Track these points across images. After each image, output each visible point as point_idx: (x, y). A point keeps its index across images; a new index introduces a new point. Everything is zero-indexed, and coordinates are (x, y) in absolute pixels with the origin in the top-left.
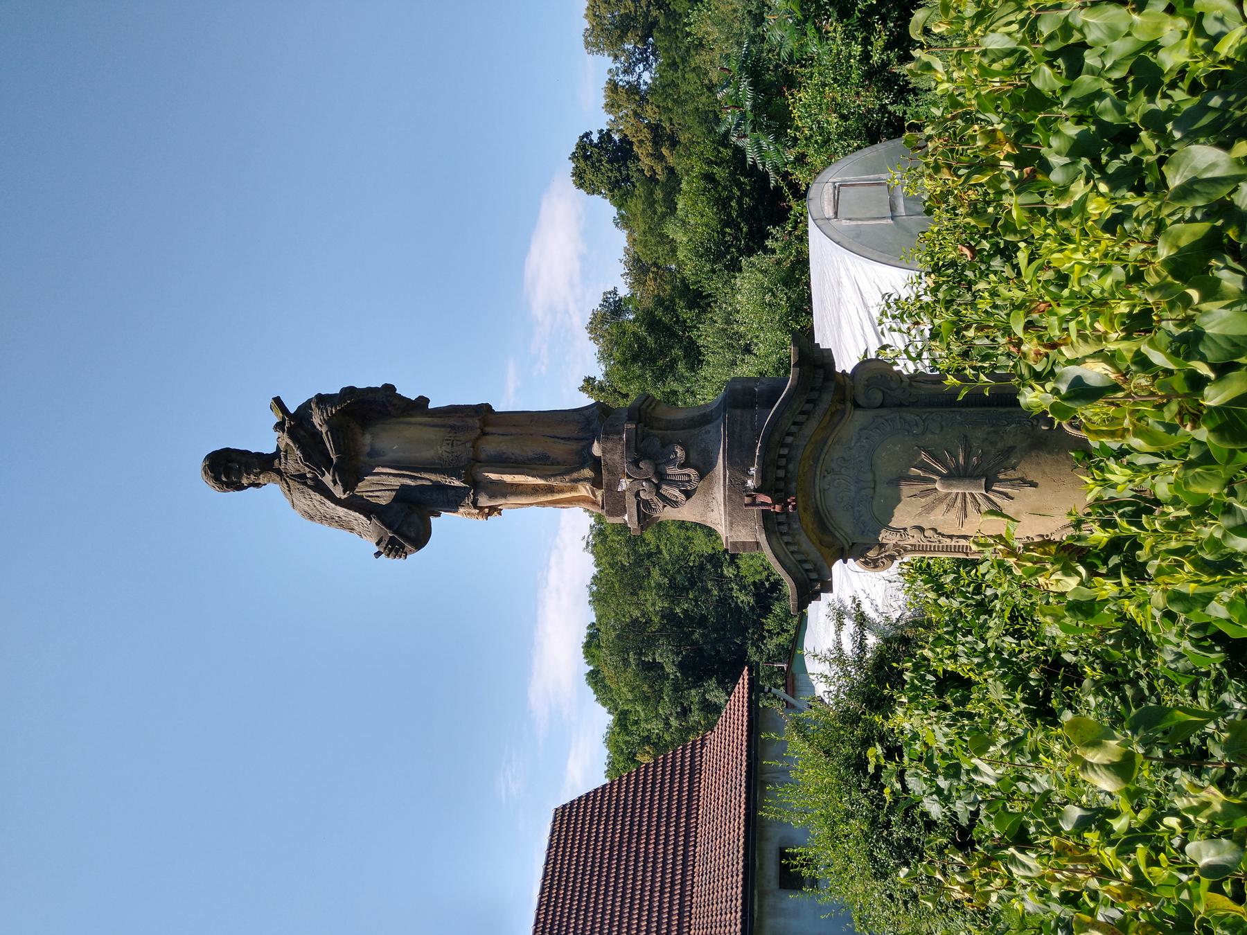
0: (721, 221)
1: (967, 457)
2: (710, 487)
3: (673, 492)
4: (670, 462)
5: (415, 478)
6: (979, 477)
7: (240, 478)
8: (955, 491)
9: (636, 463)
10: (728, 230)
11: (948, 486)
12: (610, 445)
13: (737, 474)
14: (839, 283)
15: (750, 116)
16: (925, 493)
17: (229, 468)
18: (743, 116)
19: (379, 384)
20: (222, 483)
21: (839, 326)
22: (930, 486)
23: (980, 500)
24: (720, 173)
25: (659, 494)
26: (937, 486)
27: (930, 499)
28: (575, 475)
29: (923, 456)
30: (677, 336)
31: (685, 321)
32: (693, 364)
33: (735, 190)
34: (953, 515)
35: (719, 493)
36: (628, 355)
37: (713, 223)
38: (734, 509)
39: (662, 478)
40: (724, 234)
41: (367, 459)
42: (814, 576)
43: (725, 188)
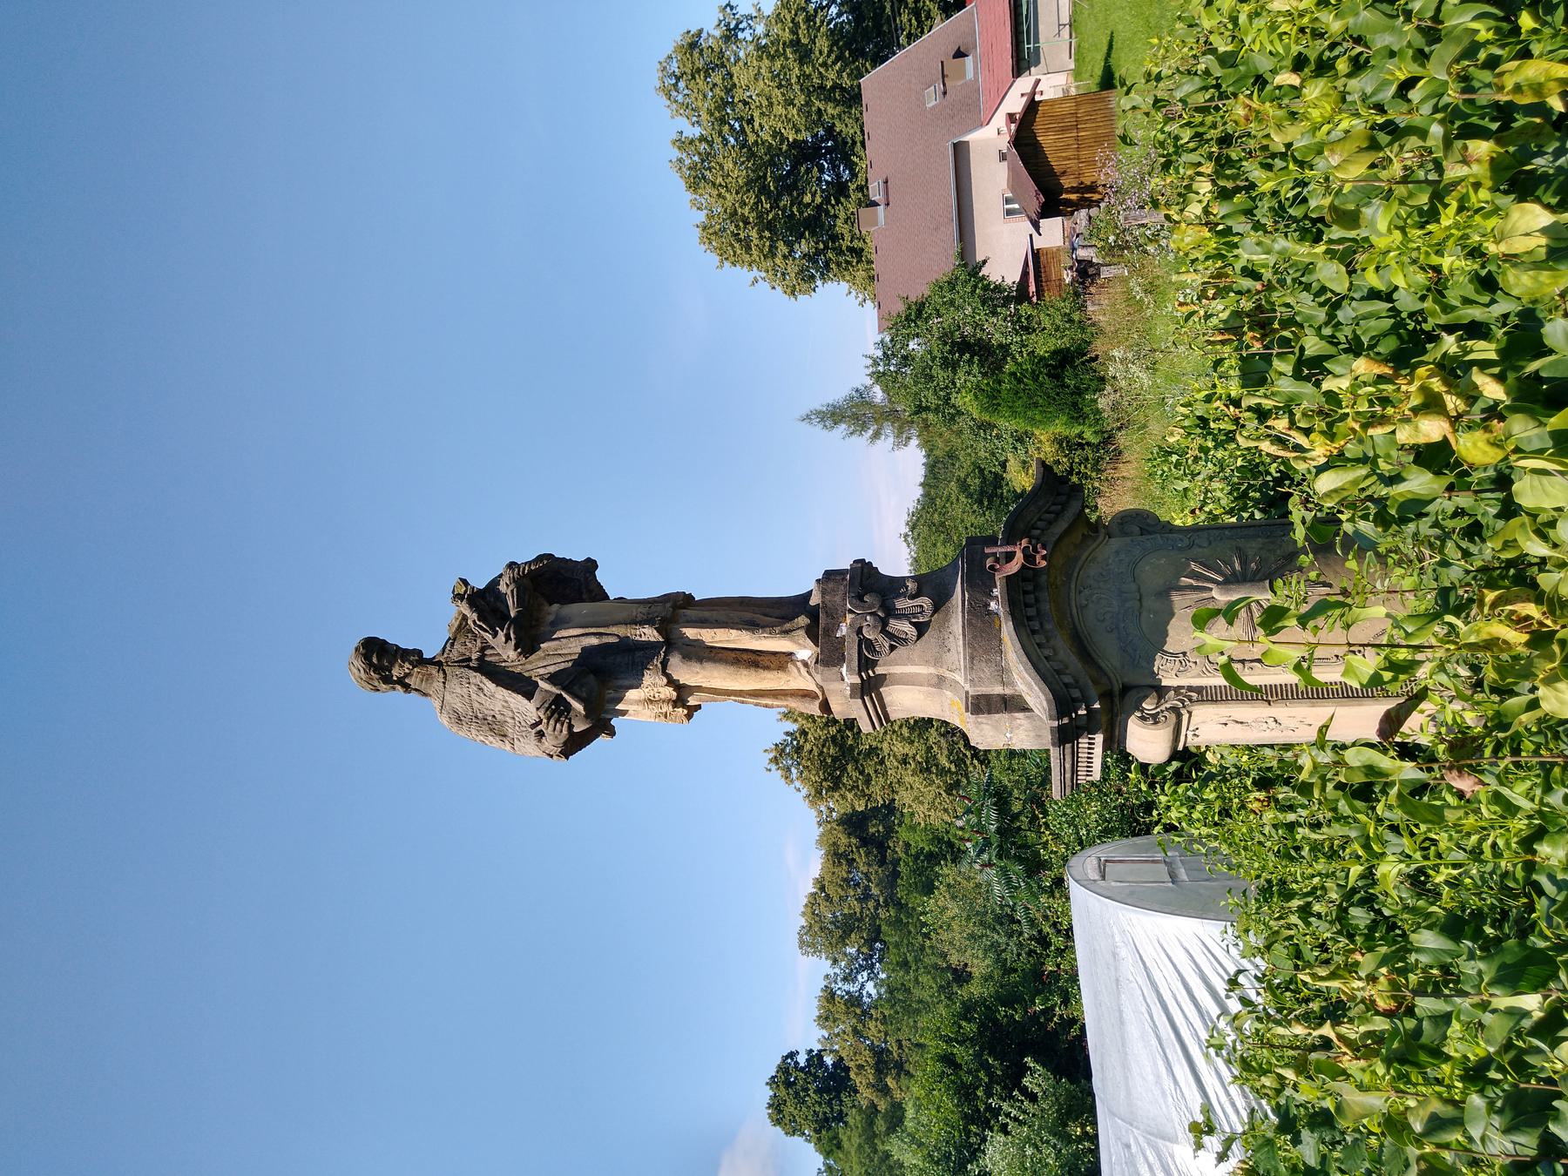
0: (965, 1117)
2: (946, 620)
3: (904, 627)
4: (899, 596)
6: (1262, 580)
7: (392, 665)
9: (860, 598)
11: (1227, 591)
14: (1115, 955)
15: (995, 840)
17: (380, 658)
19: (579, 557)
20: (371, 665)
21: (1122, 1022)
22: (1205, 595)
24: (962, 1053)
25: (884, 631)
26: (1215, 594)
28: (788, 626)
29: (1193, 565)
33: (982, 1074)
35: (957, 623)
38: (974, 637)
39: (891, 612)
40: (968, 1133)
42: (1076, 694)
43: (969, 1072)
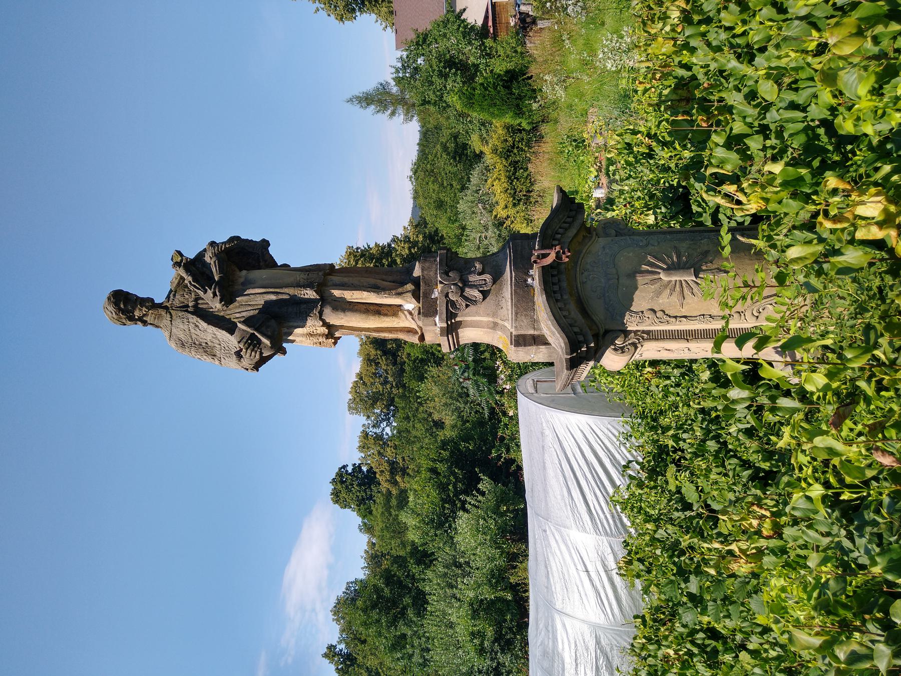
0: (442, 500)
1: (679, 257)
2: (500, 289)
3: (475, 293)
4: (471, 273)
5: (277, 293)
6: (689, 268)
7: (134, 309)
8: (674, 278)
9: (447, 273)
10: (447, 505)
11: (669, 275)
12: (427, 264)
13: (521, 274)
14: (542, 433)
15: (472, 365)
16: (653, 281)
17: (126, 305)
18: (467, 367)
19: (257, 239)
20: (120, 309)
21: (544, 468)
22: (656, 277)
23: (693, 285)
24: (442, 467)
25: (462, 296)
26: (662, 276)
27: (657, 286)
28: (400, 290)
29: (649, 258)
30: (407, 587)
31: (414, 575)
32: (420, 610)
33: (452, 478)
34: (675, 298)
35: (507, 291)
36: (368, 603)
37: (437, 501)
38: (518, 301)
39: (466, 284)
40: (444, 508)
41: (241, 287)
42: (581, 338)
43: (445, 477)
